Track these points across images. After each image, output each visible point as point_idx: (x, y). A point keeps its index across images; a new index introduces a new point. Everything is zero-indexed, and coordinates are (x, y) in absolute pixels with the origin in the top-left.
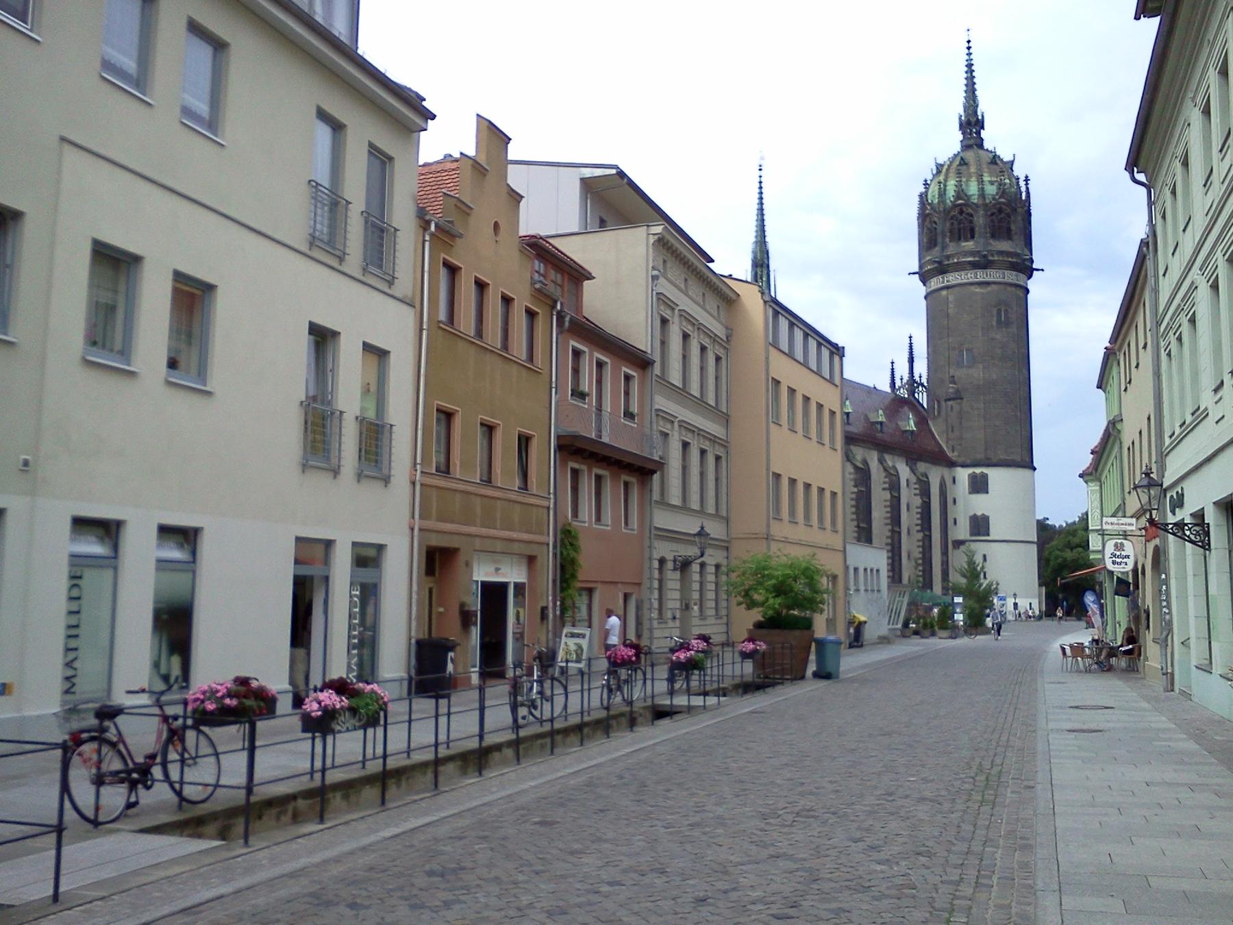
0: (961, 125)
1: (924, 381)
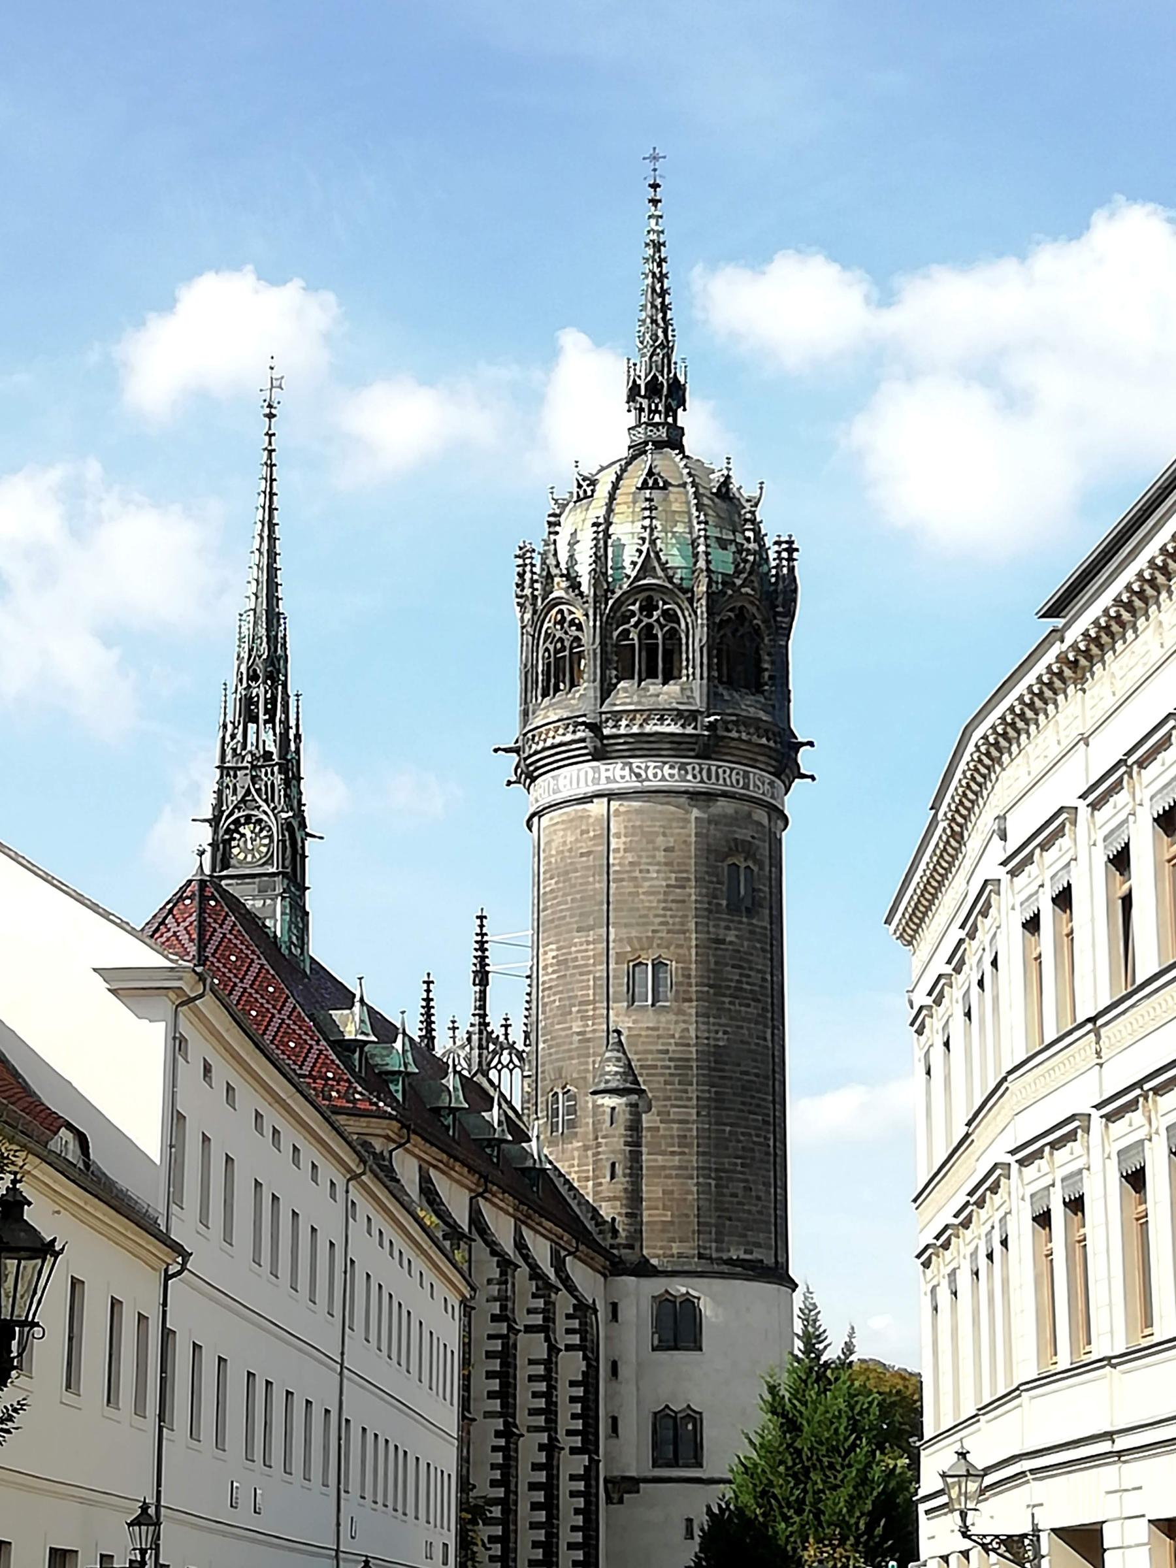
0: (633, 392)
1: (516, 1037)
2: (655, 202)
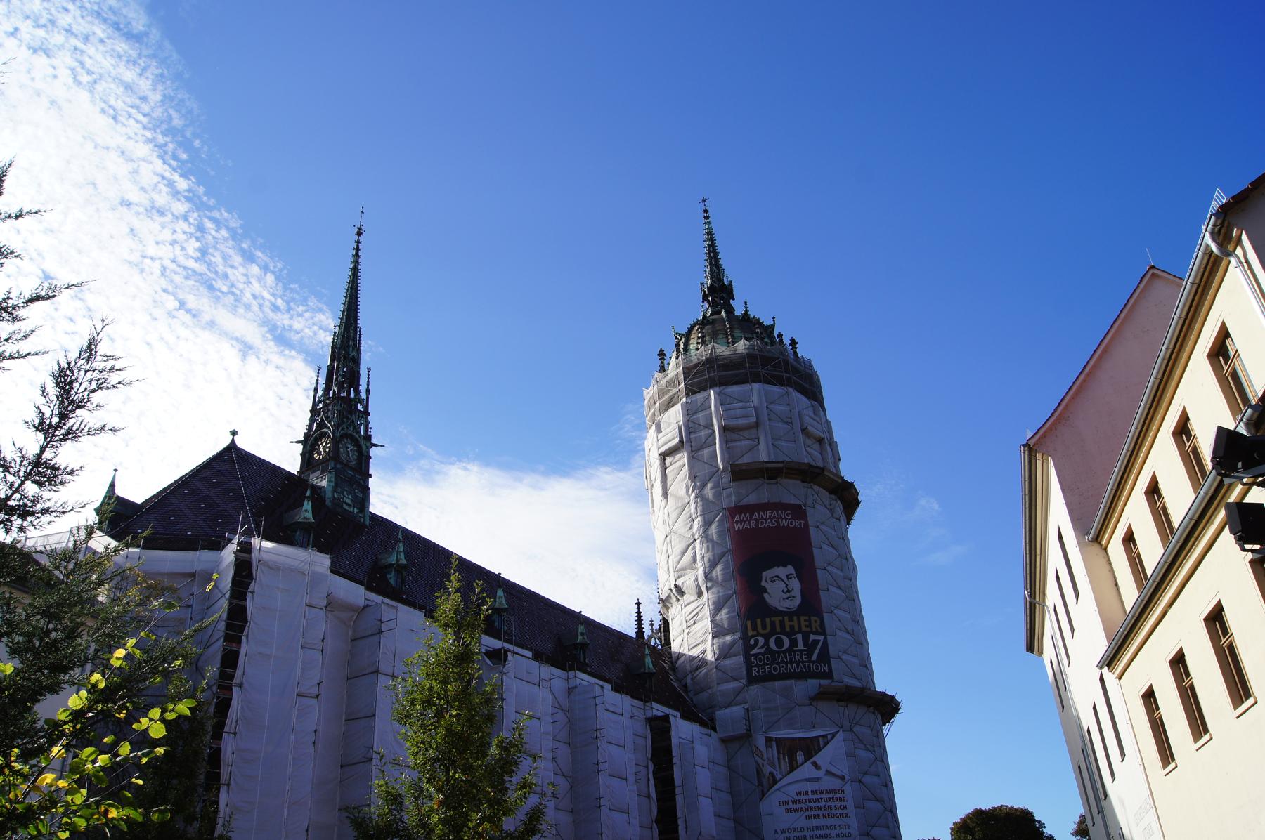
2: (707, 217)
